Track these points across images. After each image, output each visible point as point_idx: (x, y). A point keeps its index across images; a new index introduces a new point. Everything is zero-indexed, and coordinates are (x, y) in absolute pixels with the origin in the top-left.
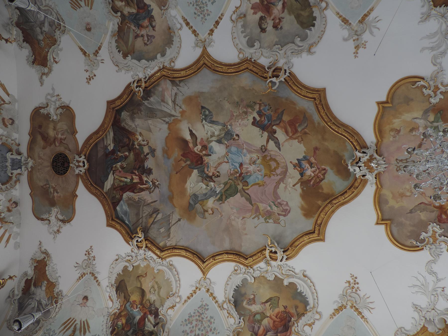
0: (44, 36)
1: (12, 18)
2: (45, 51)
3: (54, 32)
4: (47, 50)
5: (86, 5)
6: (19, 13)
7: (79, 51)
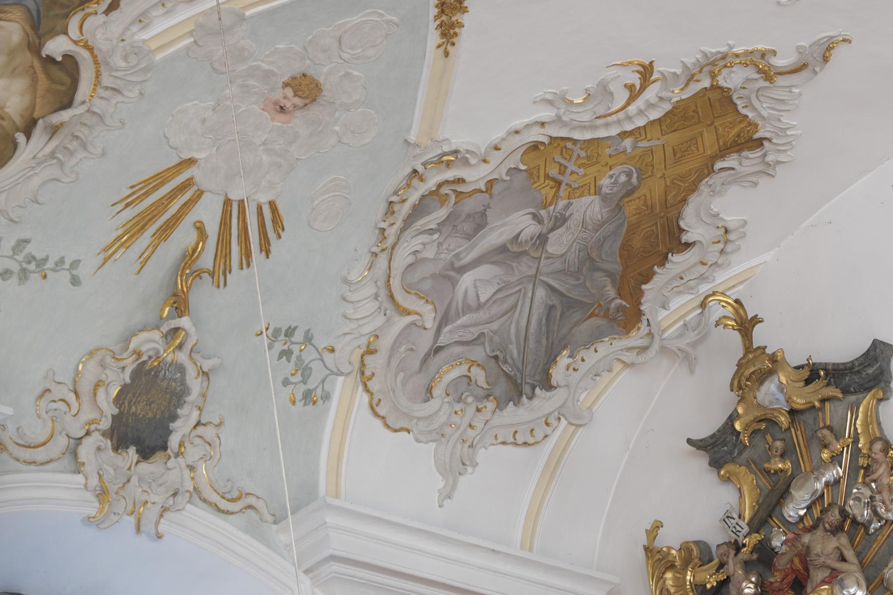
0: (562, 204)
1: (618, 360)
2: (644, 144)
3: (497, 189)
4: (628, 143)
5: (200, 194)
6: (563, 360)
7: (466, 38)
